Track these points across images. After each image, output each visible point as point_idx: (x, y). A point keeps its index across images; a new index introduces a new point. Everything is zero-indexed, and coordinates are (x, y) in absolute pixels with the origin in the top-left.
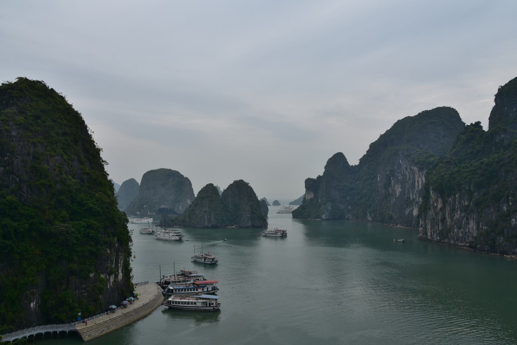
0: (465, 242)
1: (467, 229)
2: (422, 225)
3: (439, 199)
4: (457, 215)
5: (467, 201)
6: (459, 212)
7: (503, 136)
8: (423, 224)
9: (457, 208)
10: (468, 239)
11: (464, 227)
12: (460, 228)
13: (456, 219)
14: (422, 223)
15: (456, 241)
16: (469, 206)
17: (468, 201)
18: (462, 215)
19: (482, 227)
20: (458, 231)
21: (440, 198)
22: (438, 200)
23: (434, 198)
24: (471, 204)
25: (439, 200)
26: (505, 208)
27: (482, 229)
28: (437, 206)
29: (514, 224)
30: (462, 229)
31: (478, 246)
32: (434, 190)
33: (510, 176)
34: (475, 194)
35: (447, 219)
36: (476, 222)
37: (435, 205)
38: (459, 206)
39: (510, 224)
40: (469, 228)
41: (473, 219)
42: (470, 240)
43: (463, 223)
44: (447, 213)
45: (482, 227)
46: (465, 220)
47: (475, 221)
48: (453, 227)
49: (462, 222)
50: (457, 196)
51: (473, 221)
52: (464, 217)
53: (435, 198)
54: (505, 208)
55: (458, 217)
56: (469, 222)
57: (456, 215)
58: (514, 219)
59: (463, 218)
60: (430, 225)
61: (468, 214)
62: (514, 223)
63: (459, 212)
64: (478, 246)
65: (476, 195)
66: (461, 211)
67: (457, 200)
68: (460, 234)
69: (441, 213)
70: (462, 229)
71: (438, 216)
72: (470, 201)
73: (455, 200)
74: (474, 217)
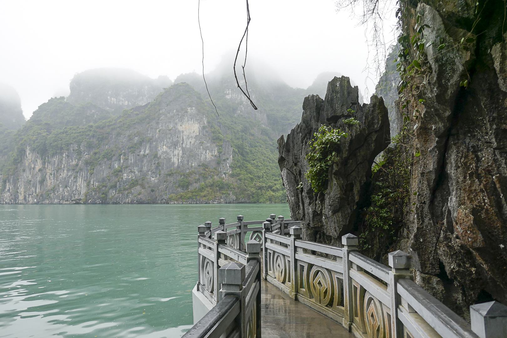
0: (71, 200)
1: (75, 187)
2: (9, 190)
3: (38, 160)
4: (64, 174)
5: (75, 160)
6: (65, 171)
7: (93, 111)
8: (10, 188)
9: (64, 167)
10: (75, 198)
11: (71, 185)
12: (66, 187)
13: (62, 178)
14: (9, 188)
15: (60, 200)
16: (77, 165)
17: (77, 160)
18: (69, 174)
19: (94, 182)
20: (63, 190)
21: (39, 159)
22: (37, 161)
23: (32, 159)
24: (80, 163)
25: (38, 161)
26: (116, 166)
27: (93, 184)
28: (34, 168)
29: (126, 179)
30: (68, 188)
31: (89, 201)
32: (33, 150)
33: (121, 138)
34: (84, 153)
35: (47, 181)
36: (84, 180)
37: (33, 166)
38: (66, 165)
39: (122, 178)
40: (76, 185)
41: (82, 177)
42: (76, 198)
43: (70, 181)
44: (48, 174)
45: (94, 182)
46: (72, 178)
47: (83, 179)
48: (59, 186)
49: (69, 181)
50: (64, 155)
51: (82, 179)
52: (71, 175)
53: (33, 159)
54: (116, 166)
55: (64, 175)
56: (77, 180)
57: (62, 174)
58: (125, 174)
59: (70, 177)
60: (23, 188)
61: (77, 172)
62: (126, 178)
63: (65, 171)
64: (89, 201)
65: (86, 154)
66: (68, 170)
67: (64, 159)
68: (66, 193)
69: (40, 174)
70: (68, 188)
71: (37, 178)
72: (79, 160)
73: (62, 160)
74: (82, 175)
